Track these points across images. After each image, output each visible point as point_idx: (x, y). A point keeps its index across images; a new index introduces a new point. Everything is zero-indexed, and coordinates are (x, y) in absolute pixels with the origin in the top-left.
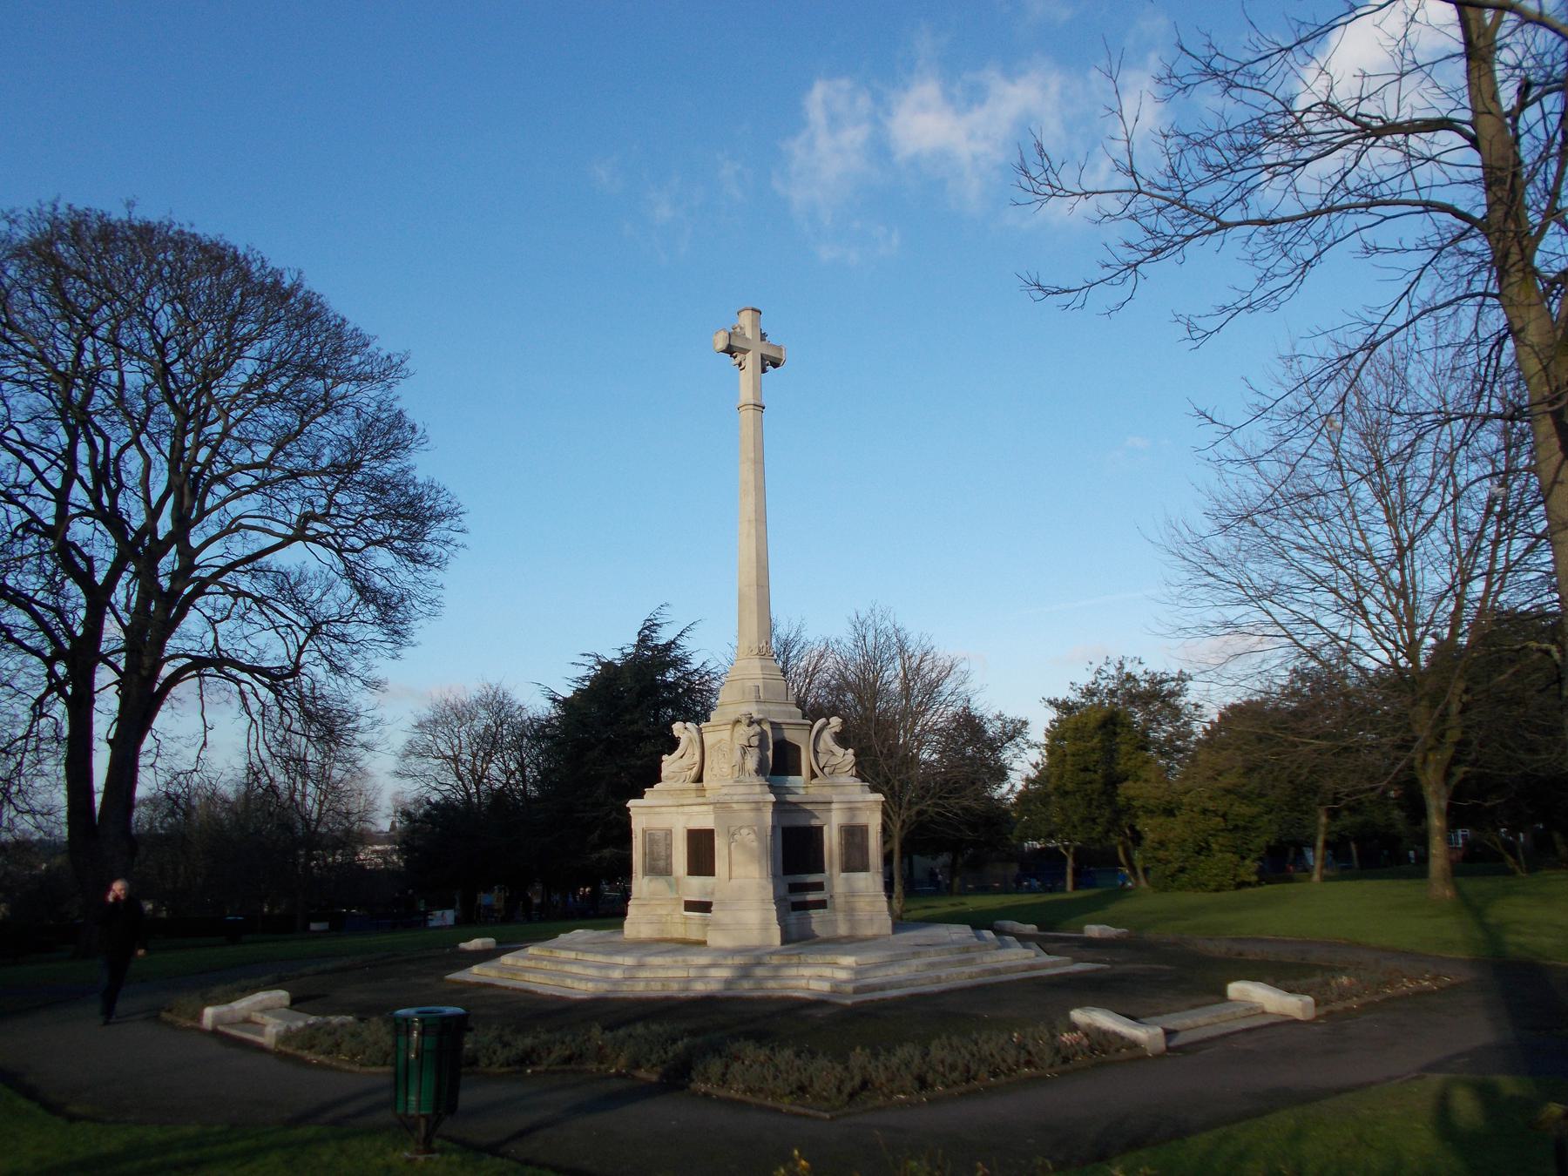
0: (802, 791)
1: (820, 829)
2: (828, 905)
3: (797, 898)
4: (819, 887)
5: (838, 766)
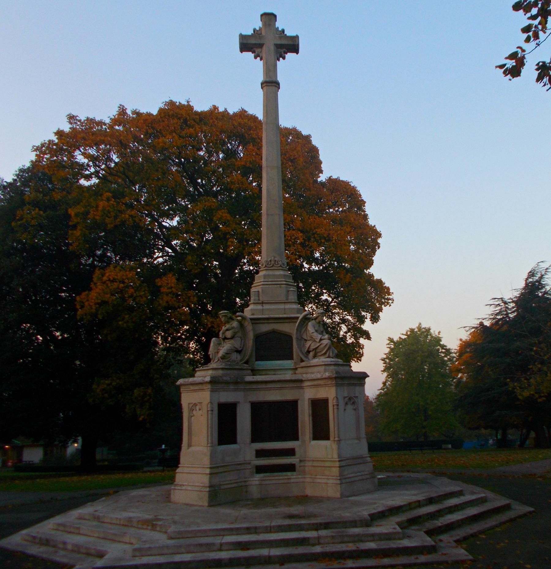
4: (291, 452)
5: (318, 350)
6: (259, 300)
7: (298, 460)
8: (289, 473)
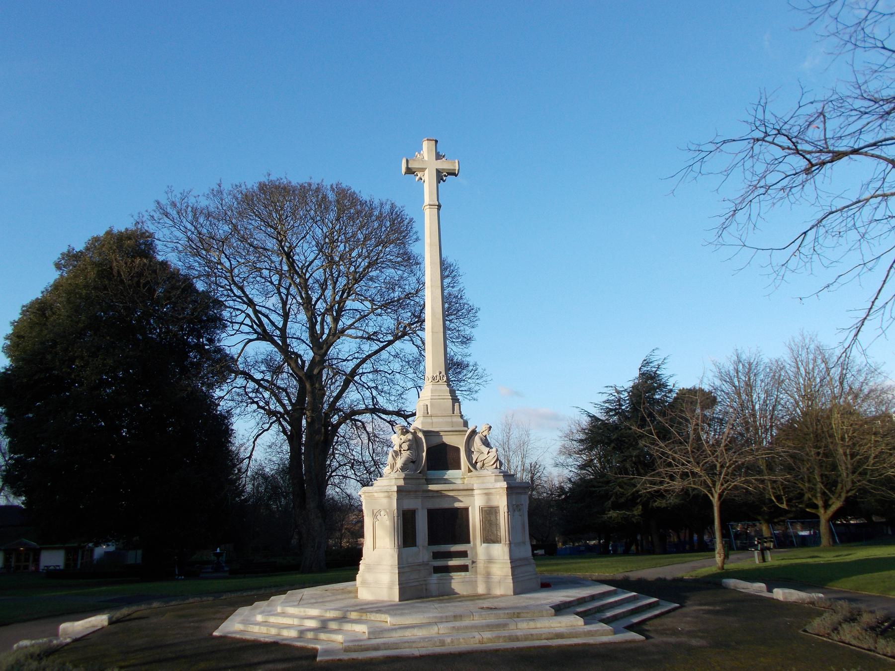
0: (459, 482)
1: (466, 510)
2: (470, 568)
3: (440, 563)
4: (464, 554)
6: (428, 413)
7: (471, 561)
8: (463, 574)
